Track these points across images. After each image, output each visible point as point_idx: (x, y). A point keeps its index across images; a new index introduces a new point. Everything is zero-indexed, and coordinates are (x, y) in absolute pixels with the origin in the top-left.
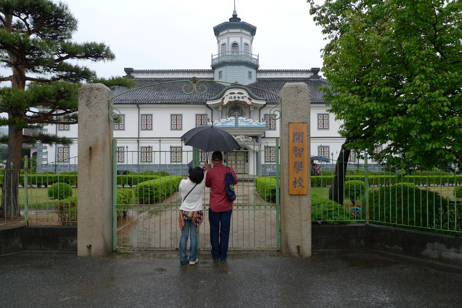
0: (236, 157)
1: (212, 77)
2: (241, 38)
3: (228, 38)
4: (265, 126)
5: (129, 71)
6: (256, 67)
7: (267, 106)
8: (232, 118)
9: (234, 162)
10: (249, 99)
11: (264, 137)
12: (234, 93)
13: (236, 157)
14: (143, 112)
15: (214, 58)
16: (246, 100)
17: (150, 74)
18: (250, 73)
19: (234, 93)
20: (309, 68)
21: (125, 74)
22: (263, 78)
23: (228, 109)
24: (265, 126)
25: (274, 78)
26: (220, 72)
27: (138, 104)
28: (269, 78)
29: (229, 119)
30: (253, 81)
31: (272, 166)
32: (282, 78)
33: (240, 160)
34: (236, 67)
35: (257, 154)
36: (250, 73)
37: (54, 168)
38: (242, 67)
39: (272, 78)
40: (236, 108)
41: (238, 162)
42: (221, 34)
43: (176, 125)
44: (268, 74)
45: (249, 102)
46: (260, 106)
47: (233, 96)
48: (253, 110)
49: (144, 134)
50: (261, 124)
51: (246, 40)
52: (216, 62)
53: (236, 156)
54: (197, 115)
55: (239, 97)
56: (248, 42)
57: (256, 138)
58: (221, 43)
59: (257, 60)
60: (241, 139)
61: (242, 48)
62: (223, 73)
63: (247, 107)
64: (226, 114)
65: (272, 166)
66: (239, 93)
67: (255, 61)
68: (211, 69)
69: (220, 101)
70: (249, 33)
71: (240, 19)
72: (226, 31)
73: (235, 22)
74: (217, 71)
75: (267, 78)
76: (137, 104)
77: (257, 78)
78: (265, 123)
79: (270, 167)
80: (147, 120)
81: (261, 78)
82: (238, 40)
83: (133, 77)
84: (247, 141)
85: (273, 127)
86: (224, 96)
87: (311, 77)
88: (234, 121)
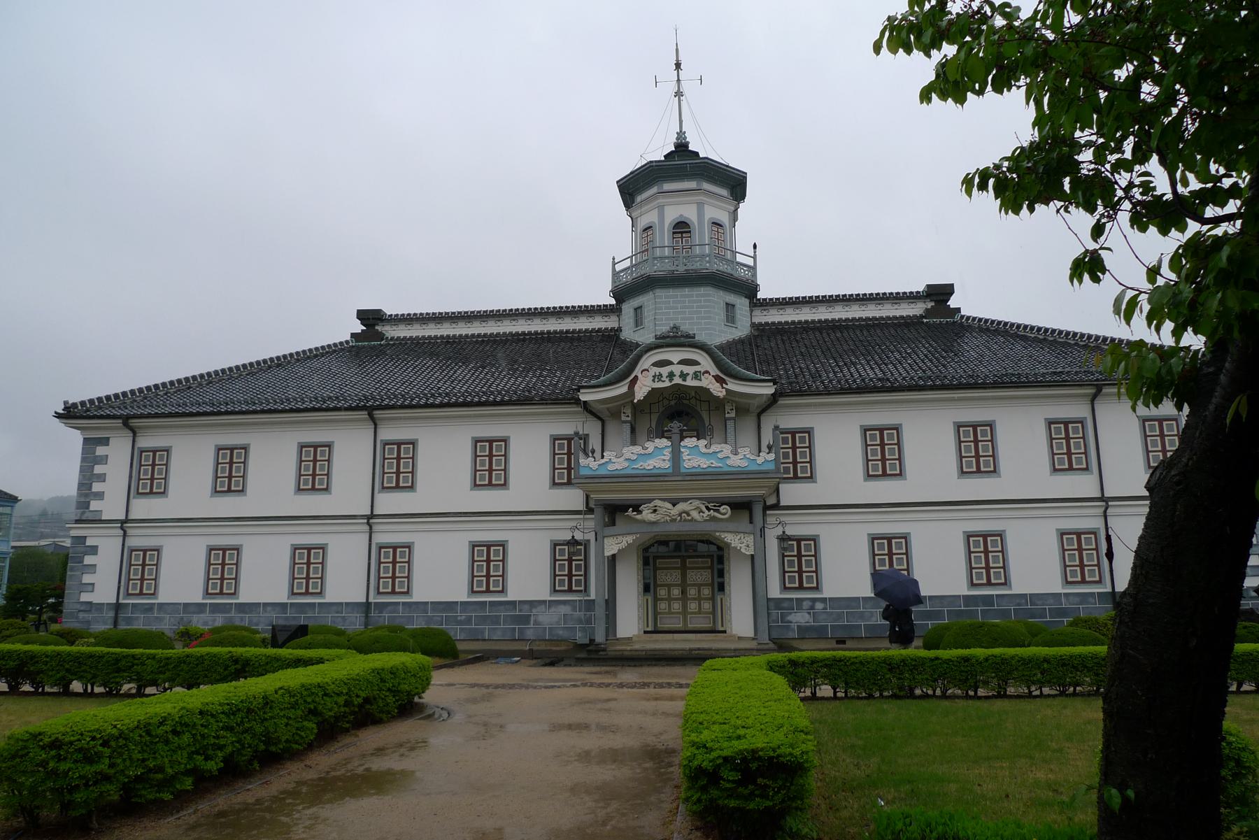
0: (684, 576)
1: (616, 325)
2: (700, 205)
3: (661, 209)
4: (772, 467)
5: (370, 318)
6: (748, 289)
7: (782, 401)
8: (664, 442)
9: (676, 592)
10: (717, 378)
11: (776, 506)
12: (669, 363)
13: (684, 576)
14: (387, 433)
15: (618, 268)
16: (708, 383)
17: (432, 325)
18: (730, 307)
19: (669, 363)
20: (920, 287)
21: (359, 327)
22: (773, 323)
23: (655, 417)
24: (772, 467)
25: (806, 322)
26: (638, 310)
27: (370, 411)
28: (793, 322)
29: (650, 446)
30: (742, 330)
31: (806, 605)
32: (833, 320)
33: (700, 586)
34: (687, 291)
35: (755, 563)
36: (730, 307)
37: (112, 614)
38: (703, 290)
39: (800, 322)
40: (680, 412)
41: (692, 592)
42: (639, 199)
43: (490, 470)
44: (789, 310)
45: (717, 390)
46: (756, 402)
47: (665, 371)
48: (733, 415)
49: (390, 503)
50: (760, 460)
52: (626, 278)
53: (684, 569)
54: (555, 439)
55: (683, 376)
56: (724, 218)
57: (742, 507)
58: (643, 222)
59: (753, 269)
60: (695, 514)
61: (701, 235)
62: (645, 310)
63: (717, 408)
64: (649, 432)
65: (806, 605)
66: (682, 362)
67: (743, 273)
68: (613, 302)
69: (622, 389)
70: (724, 192)
71: (697, 154)
72: (654, 190)
73: (683, 164)
74: (628, 308)
75: (787, 323)
76: (371, 410)
77: (753, 325)
78: (772, 456)
79: (800, 608)
80: (399, 458)
81: (767, 324)
82: (688, 212)
83: (381, 336)
84: (713, 519)
85: (804, 470)
86: (637, 372)
87: (928, 313)
88: (667, 454)
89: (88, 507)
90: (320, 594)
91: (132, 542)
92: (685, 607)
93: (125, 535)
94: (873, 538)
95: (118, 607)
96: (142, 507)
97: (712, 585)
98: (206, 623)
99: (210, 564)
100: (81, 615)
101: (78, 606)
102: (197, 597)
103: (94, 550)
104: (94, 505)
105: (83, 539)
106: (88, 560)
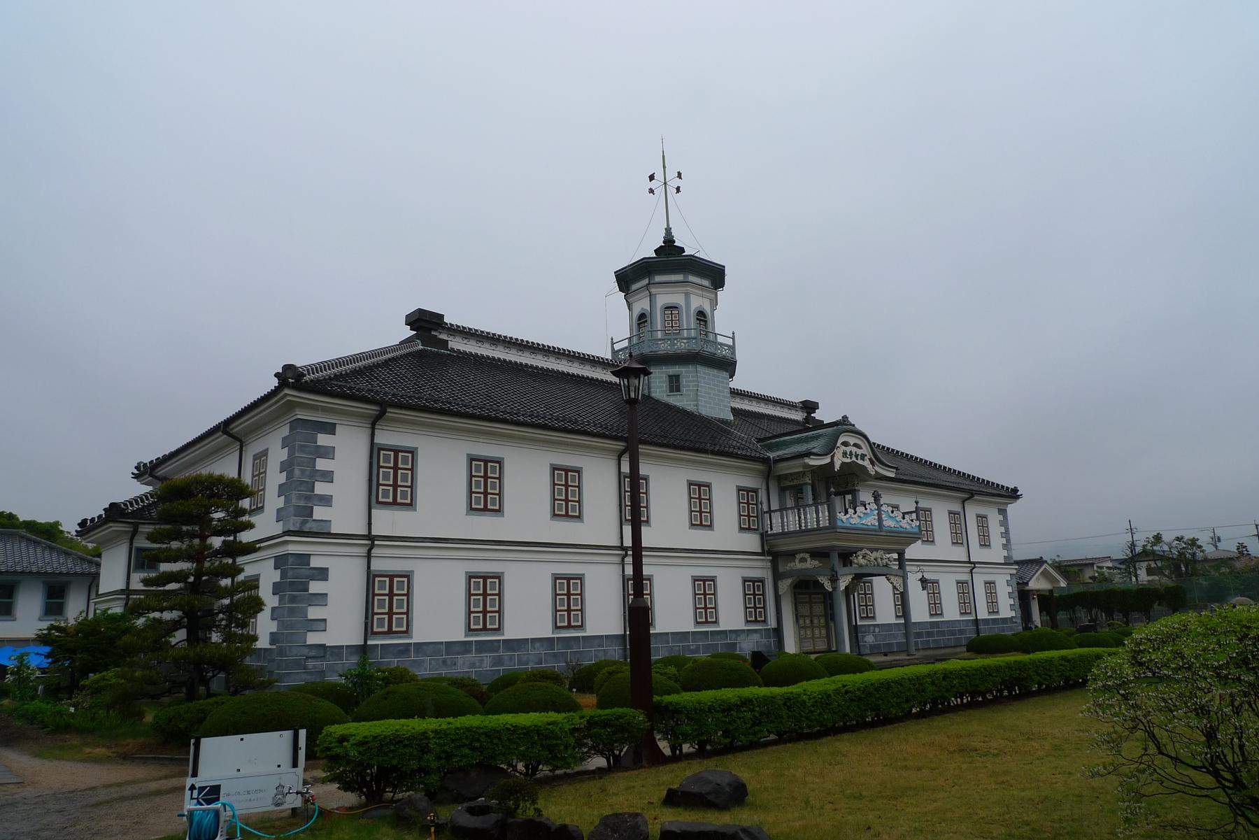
0: (811, 608)
2: (687, 295)
3: (687, 295)
13: (811, 608)
16: (866, 463)
17: (473, 342)
34: (715, 372)
41: (816, 621)
51: (698, 302)
66: (855, 445)
71: (682, 250)
89: (311, 515)
90: (716, 622)
91: (377, 565)
92: (813, 633)
93: (369, 557)
94: (470, 576)
95: (363, 649)
96: (387, 522)
97: (826, 616)
98: (473, 665)
99: (470, 595)
100: (310, 663)
101: (306, 651)
102: (459, 635)
103: (322, 574)
104: (319, 513)
105: (305, 558)
106: (315, 587)
